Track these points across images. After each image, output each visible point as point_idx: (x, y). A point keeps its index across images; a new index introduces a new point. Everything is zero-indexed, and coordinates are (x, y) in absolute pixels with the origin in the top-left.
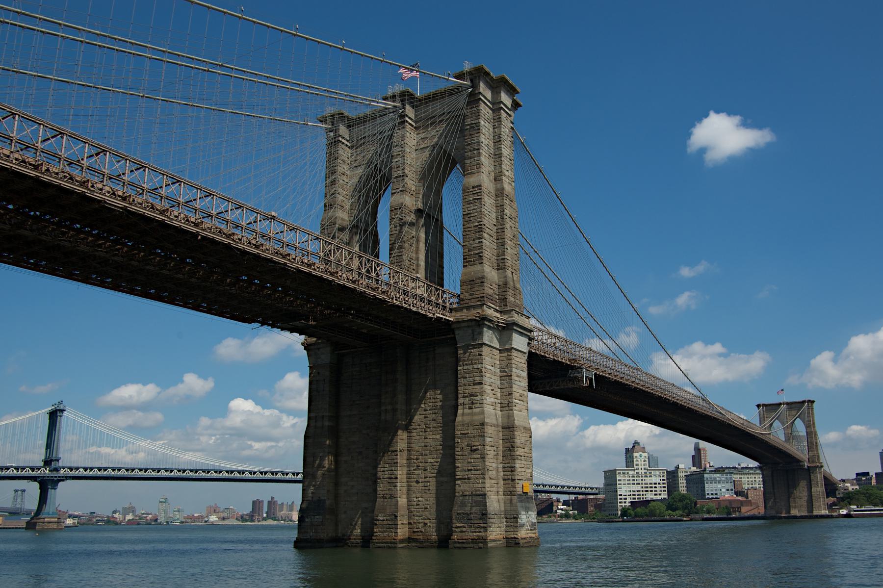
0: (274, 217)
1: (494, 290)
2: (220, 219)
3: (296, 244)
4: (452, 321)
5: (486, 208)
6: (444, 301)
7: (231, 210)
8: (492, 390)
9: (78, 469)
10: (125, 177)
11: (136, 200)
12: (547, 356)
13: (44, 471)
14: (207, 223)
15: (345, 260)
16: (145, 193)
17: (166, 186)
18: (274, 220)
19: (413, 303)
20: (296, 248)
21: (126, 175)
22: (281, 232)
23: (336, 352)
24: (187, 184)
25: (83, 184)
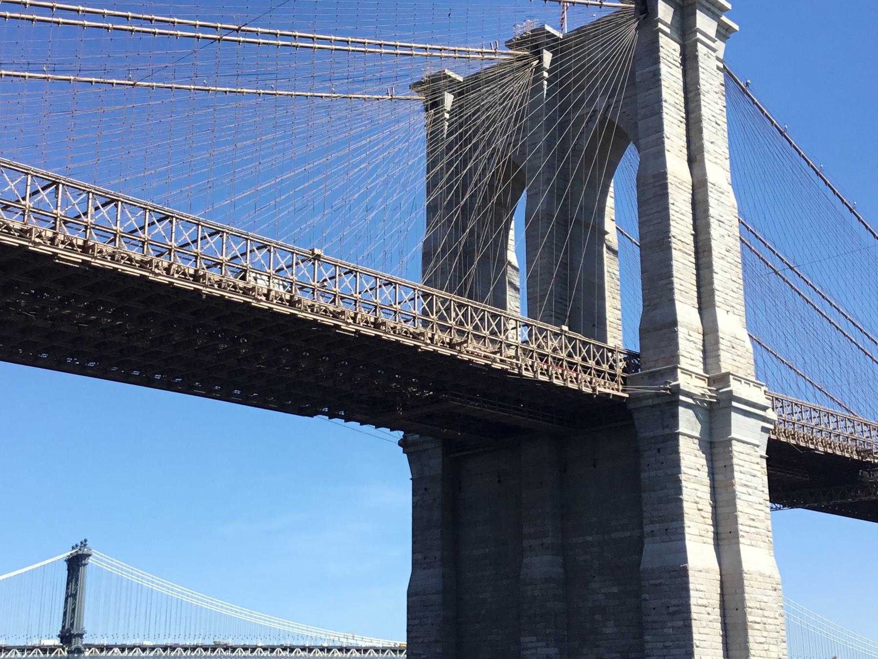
0: (319, 256)
1: (695, 343)
2: (234, 267)
3: (355, 295)
4: (627, 398)
5: (677, 209)
6: (611, 367)
7: (251, 251)
8: (699, 510)
9: (112, 649)
10: (87, 218)
11: (104, 251)
12: (812, 447)
13: (61, 653)
14: (214, 275)
15: (437, 313)
16: (117, 239)
17: (149, 225)
18: (319, 260)
19: (556, 373)
20: (356, 301)
21: (89, 215)
22: (330, 279)
23: (451, 456)
24: (181, 219)
25: (23, 233)
